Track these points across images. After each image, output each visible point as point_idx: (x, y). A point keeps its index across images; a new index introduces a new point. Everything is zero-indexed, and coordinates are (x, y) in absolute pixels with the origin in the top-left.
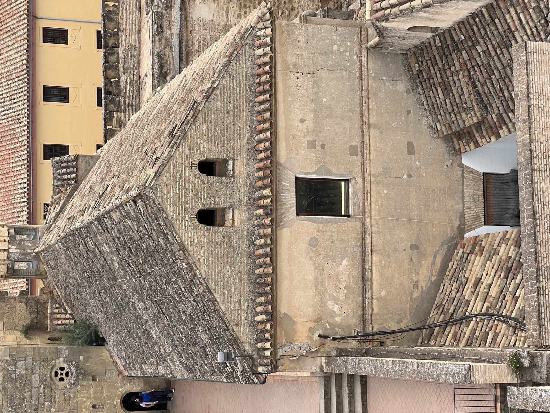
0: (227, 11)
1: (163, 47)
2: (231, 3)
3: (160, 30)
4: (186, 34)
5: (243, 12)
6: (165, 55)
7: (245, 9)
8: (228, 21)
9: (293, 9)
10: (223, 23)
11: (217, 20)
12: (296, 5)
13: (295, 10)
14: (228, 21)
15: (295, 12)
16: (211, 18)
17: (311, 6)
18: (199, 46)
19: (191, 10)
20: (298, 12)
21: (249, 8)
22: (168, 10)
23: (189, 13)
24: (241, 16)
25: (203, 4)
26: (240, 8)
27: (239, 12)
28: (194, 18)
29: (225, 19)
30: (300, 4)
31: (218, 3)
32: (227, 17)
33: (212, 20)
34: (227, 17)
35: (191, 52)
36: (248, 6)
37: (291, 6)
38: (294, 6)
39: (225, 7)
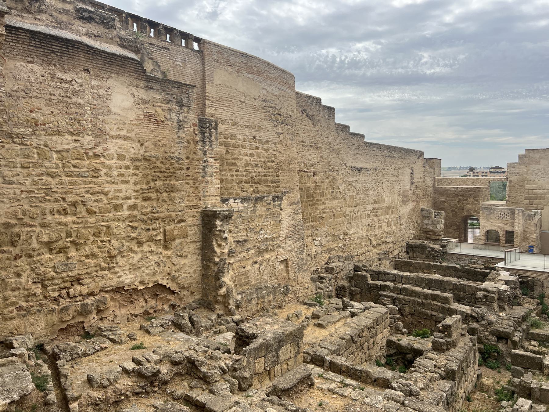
0: (126, 138)
1: (54, 14)
2: (139, 145)
3: (86, 15)
4: (83, 60)
5: (127, 163)
6: (40, 11)
7: (132, 168)
8: (112, 137)
9: (140, 244)
10: (107, 130)
11: (109, 118)
12: (145, 248)
13: (138, 247)
14: (112, 137)
15: (135, 248)
16: (113, 110)
17: (147, 272)
18: (62, 81)
19: (122, 78)
20: (136, 253)
21: (135, 174)
22: (118, 40)
23: (118, 74)
24: (122, 160)
25: (132, 99)
26: (133, 160)
27: (127, 156)
28: (110, 82)
29: (113, 133)
30: (148, 254)
31: (136, 125)
32: (119, 137)
33: (109, 111)
34: (119, 137)
35: (49, 63)
36: (137, 171)
37: (144, 240)
38: (145, 246)
39: (132, 135)
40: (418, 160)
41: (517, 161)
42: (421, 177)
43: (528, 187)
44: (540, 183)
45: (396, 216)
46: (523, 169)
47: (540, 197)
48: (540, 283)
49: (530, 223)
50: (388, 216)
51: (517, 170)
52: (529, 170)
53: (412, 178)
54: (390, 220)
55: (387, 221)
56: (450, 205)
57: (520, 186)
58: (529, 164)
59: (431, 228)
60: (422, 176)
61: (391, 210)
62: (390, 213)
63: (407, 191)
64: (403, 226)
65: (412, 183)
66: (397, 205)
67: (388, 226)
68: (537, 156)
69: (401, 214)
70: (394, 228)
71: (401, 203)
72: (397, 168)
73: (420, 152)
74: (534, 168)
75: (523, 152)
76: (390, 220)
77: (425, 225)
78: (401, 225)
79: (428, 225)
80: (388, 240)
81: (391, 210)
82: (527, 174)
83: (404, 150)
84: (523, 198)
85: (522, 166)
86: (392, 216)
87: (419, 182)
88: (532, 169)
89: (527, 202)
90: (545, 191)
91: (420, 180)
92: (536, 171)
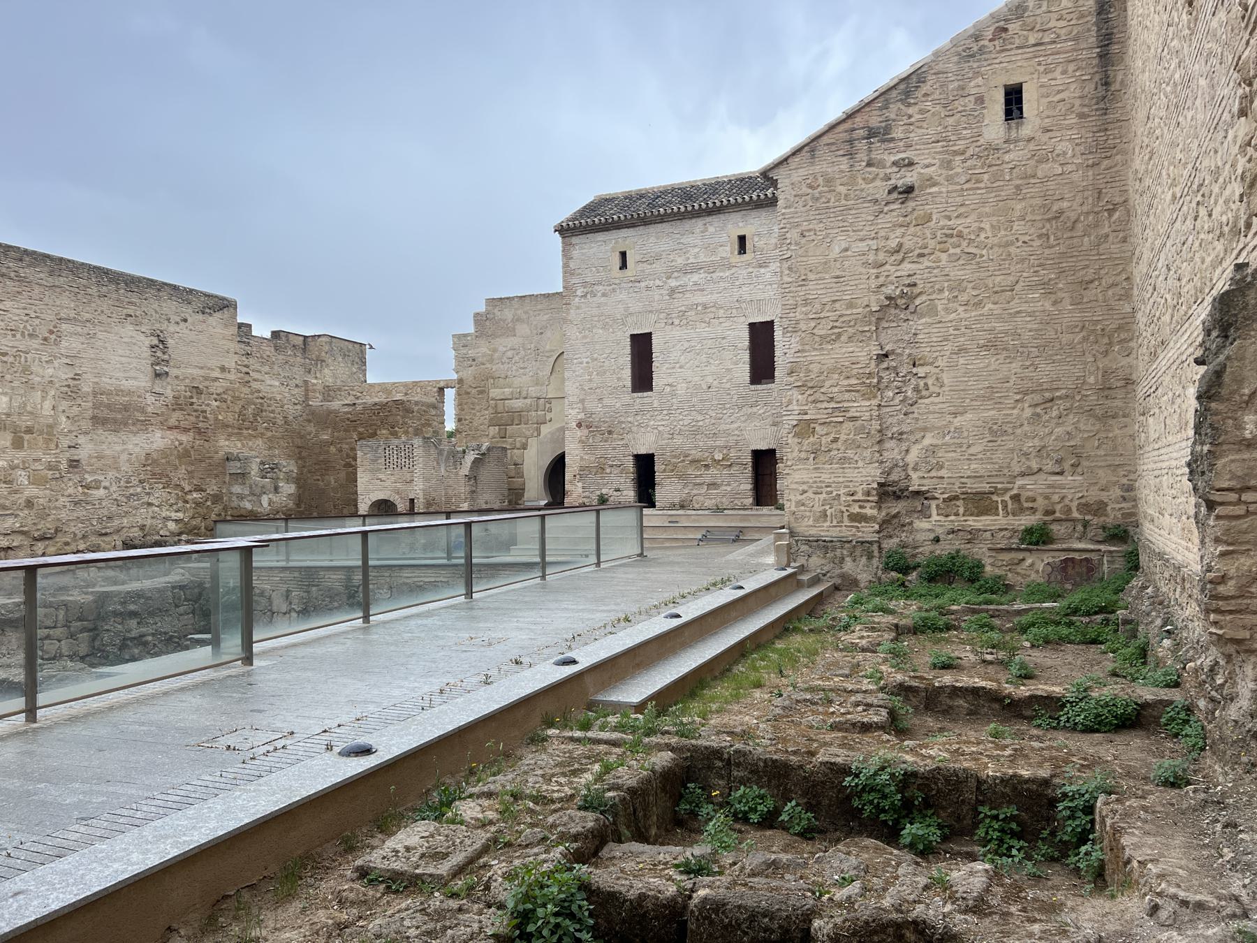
41: (471, 329)
43: (494, 393)
44: (517, 381)
46: (483, 349)
47: (516, 417)
48: (264, 601)
49: (457, 474)
51: (471, 353)
52: (495, 350)
56: (340, 451)
57: (481, 392)
58: (494, 336)
59: (248, 506)
68: (508, 314)
74: (504, 344)
75: (482, 308)
77: (234, 498)
79: (241, 497)
82: (491, 361)
83: (106, 272)
84: (486, 422)
85: (482, 342)
88: (501, 349)
89: (494, 430)
90: (528, 401)
92: (510, 354)
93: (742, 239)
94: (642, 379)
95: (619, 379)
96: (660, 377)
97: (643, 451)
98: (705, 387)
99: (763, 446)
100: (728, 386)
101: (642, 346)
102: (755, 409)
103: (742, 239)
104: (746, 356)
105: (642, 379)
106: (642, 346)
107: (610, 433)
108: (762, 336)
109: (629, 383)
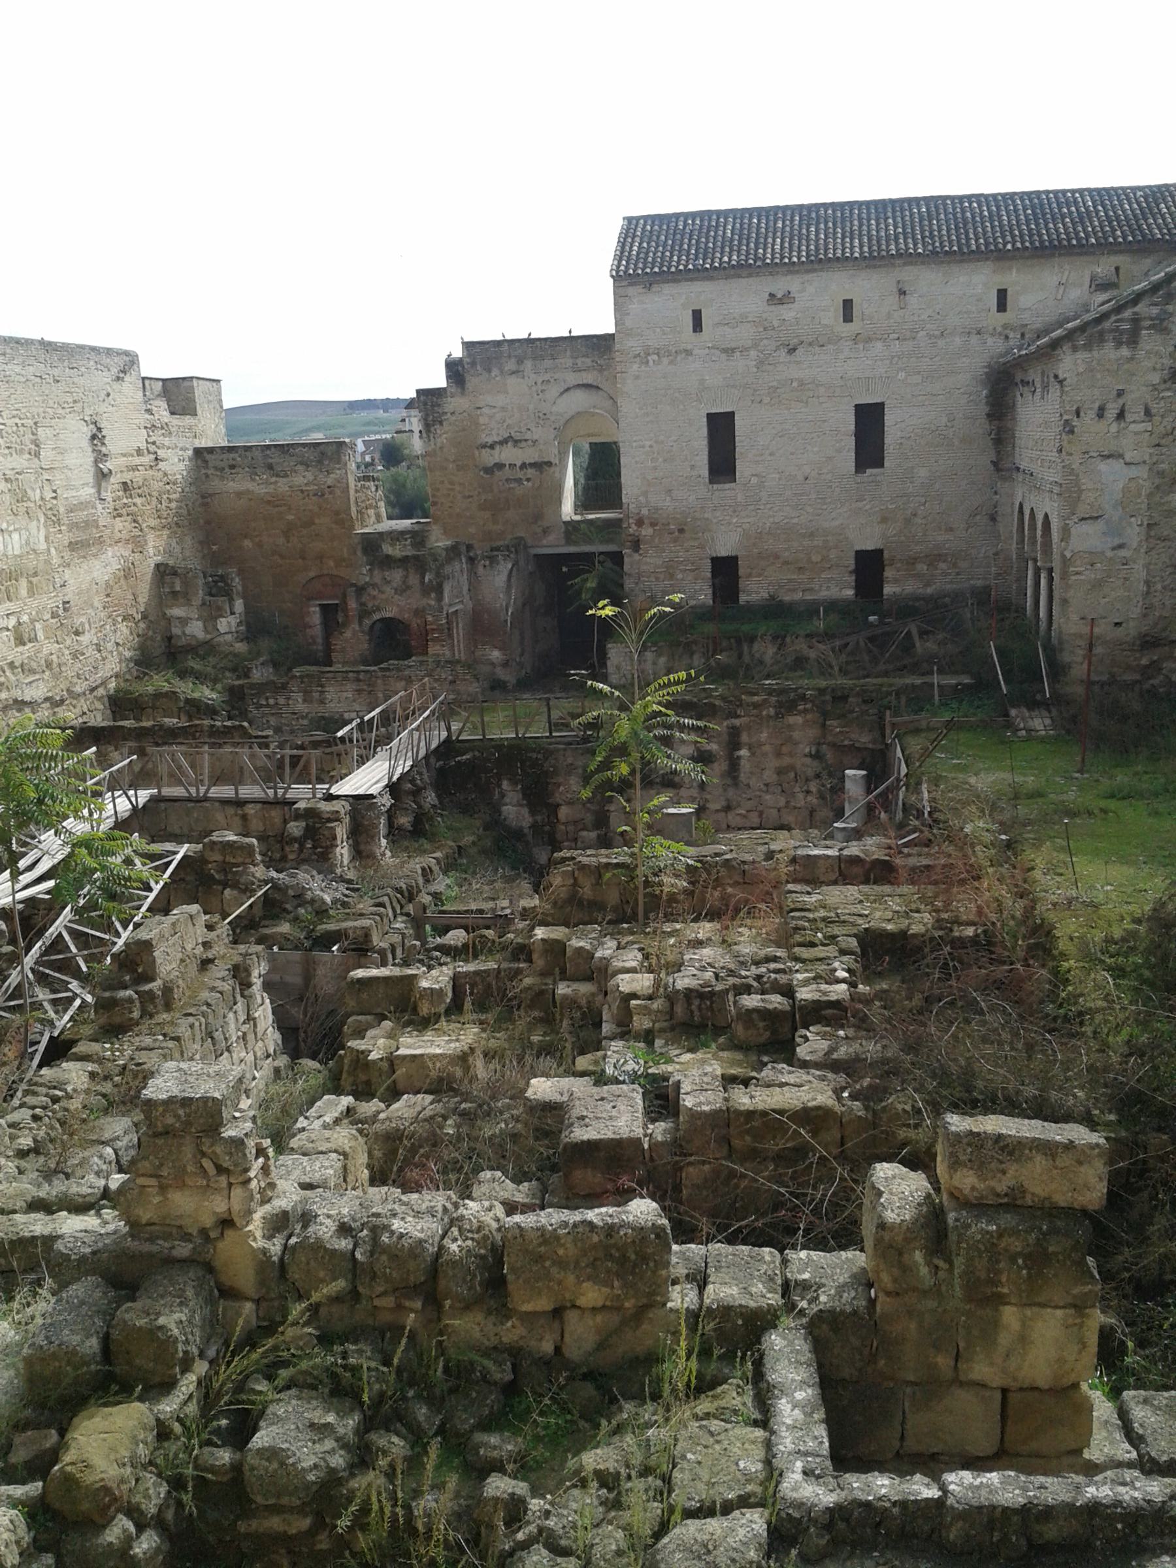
40: (116, 385)
42: (139, 452)
45: (49, 601)
50: (12, 606)
53: (100, 457)
54: (25, 618)
55: (12, 622)
60: (143, 446)
61: (23, 583)
62: (24, 592)
63: (83, 505)
64: (85, 639)
65: (102, 476)
66: (48, 562)
67: (20, 641)
69: (70, 593)
70: (48, 647)
71: (67, 555)
72: (30, 422)
73: (127, 353)
76: (25, 618)
78: (77, 633)
80: (29, 694)
81: (23, 583)
86: (34, 603)
87: (134, 468)
91: (137, 460)
93: (848, 305)
94: (722, 464)
95: (692, 467)
96: (743, 468)
97: (723, 553)
98: (801, 478)
99: (869, 546)
100: (829, 477)
101: (721, 429)
102: (860, 504)
103: (848, 305)
104: (851, 442)
105: (722, 464)
106: (721, 429)
107: (681, 531)
108: (869, 420)
109: (705, 472)
